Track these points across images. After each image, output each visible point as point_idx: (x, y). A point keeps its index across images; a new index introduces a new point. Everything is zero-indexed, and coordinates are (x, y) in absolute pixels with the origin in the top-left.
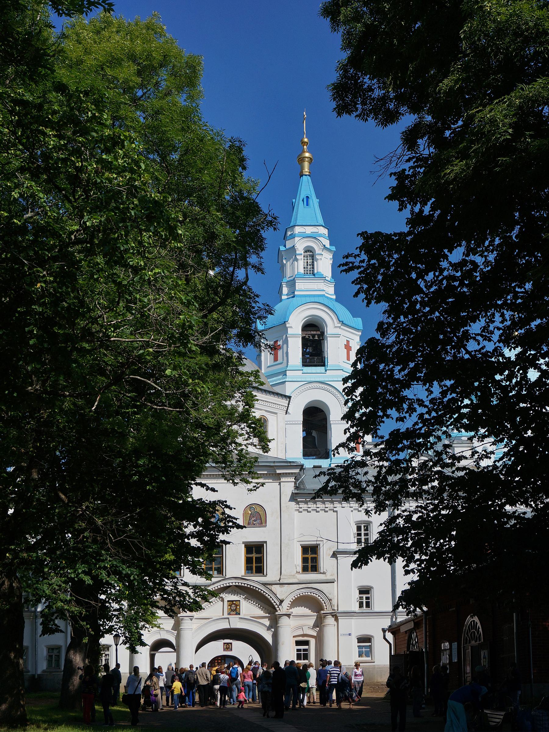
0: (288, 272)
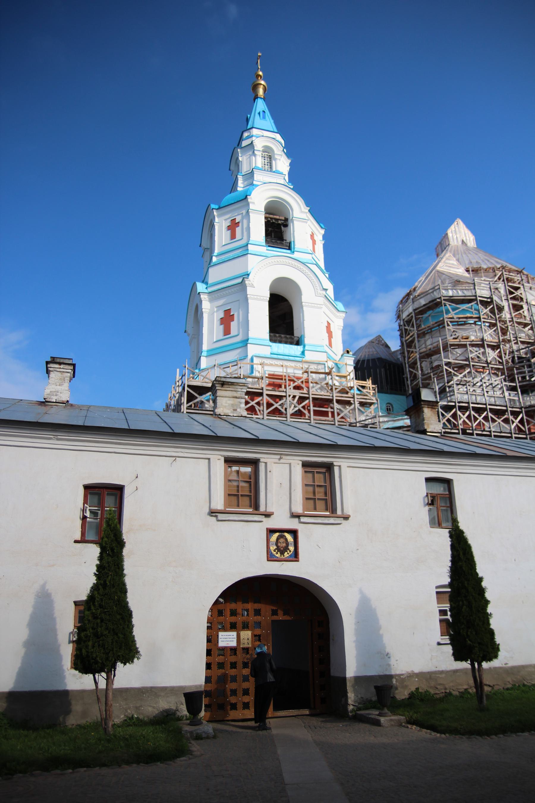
0: (245, 168)
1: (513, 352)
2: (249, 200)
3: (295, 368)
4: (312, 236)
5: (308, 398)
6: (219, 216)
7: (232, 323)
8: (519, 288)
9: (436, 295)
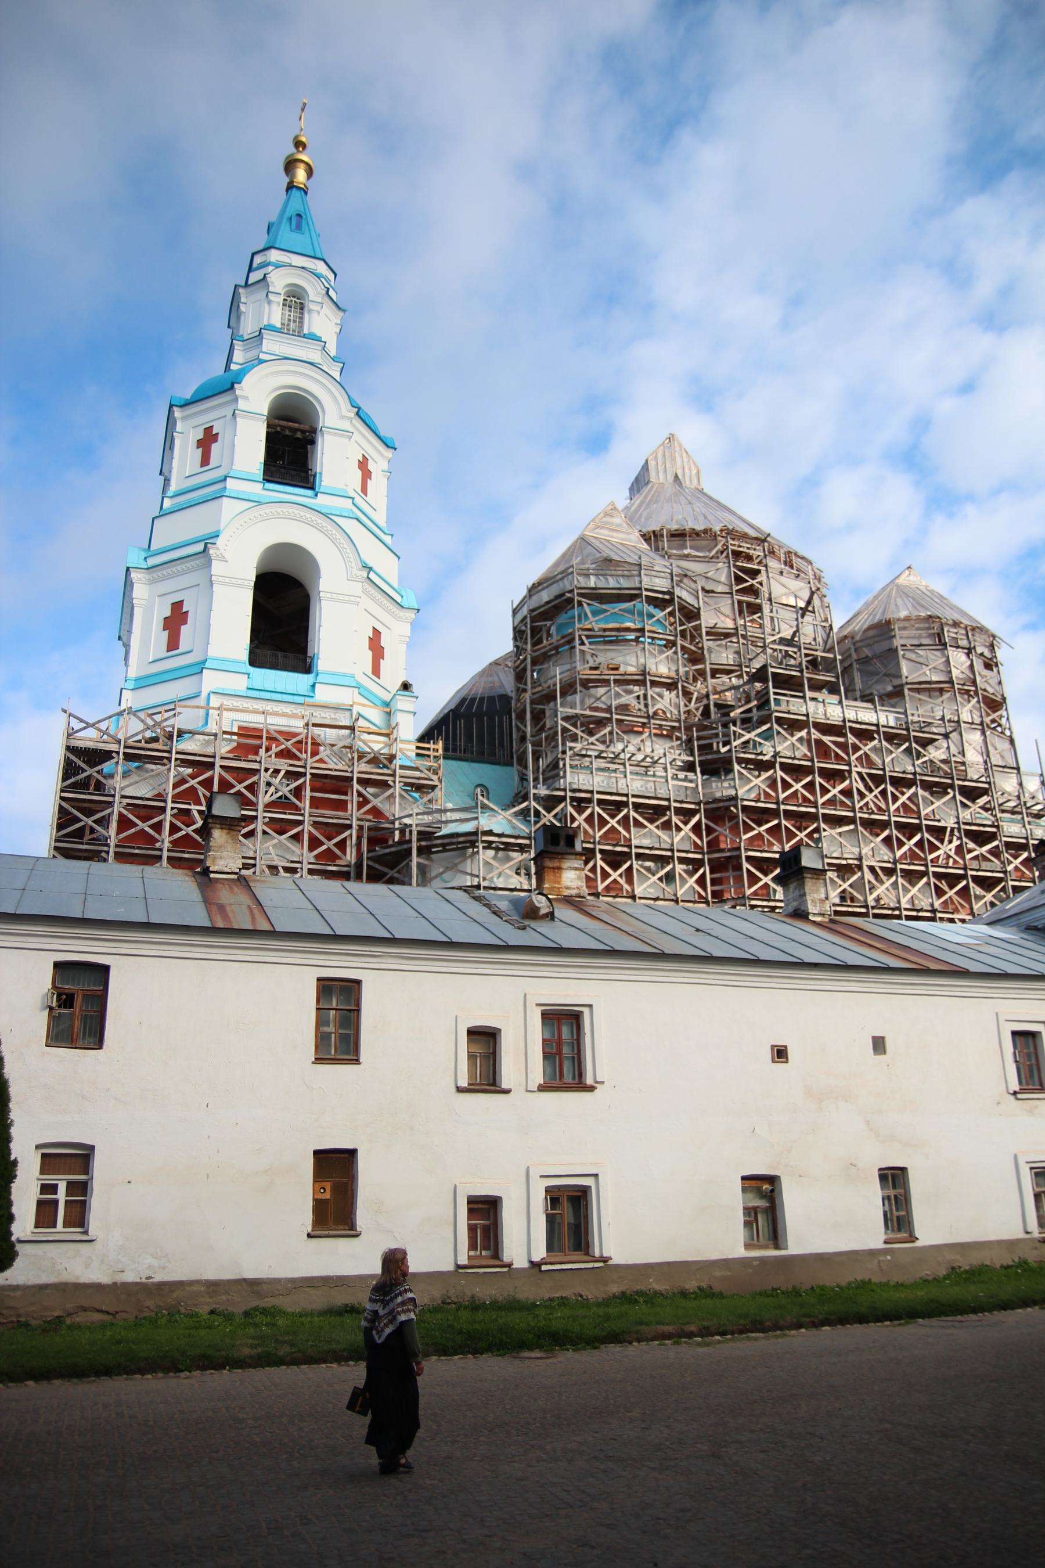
1: (707, 696)
2: (238, 392)
3: (294, 716)
4: (363, 464)
5: (304, 774)
6: (184, 418)
7: (183, 628)
8: (758, 572)
9: (567, 585)
